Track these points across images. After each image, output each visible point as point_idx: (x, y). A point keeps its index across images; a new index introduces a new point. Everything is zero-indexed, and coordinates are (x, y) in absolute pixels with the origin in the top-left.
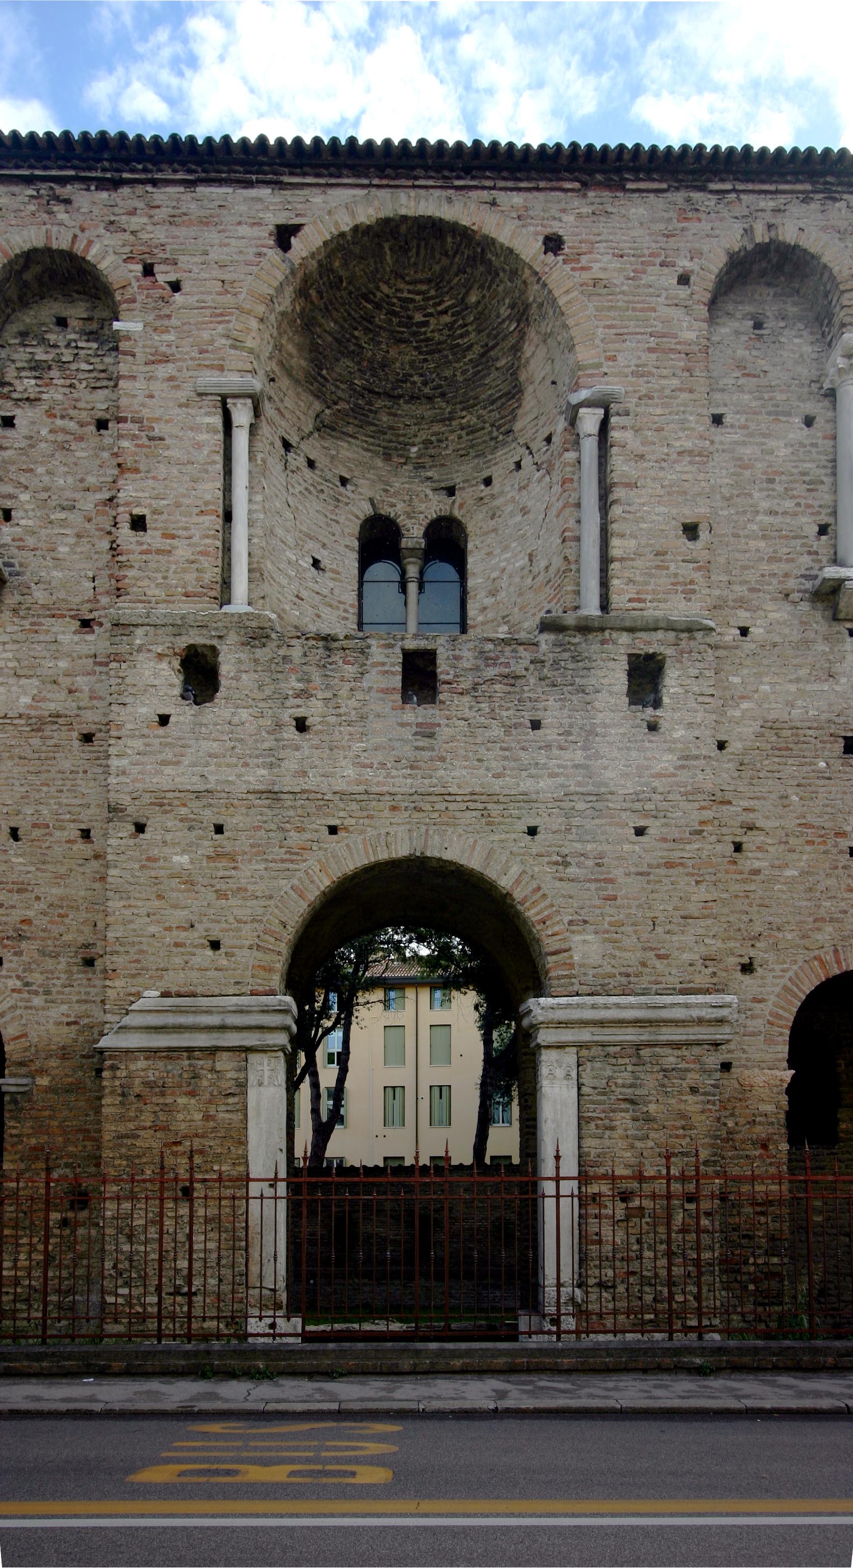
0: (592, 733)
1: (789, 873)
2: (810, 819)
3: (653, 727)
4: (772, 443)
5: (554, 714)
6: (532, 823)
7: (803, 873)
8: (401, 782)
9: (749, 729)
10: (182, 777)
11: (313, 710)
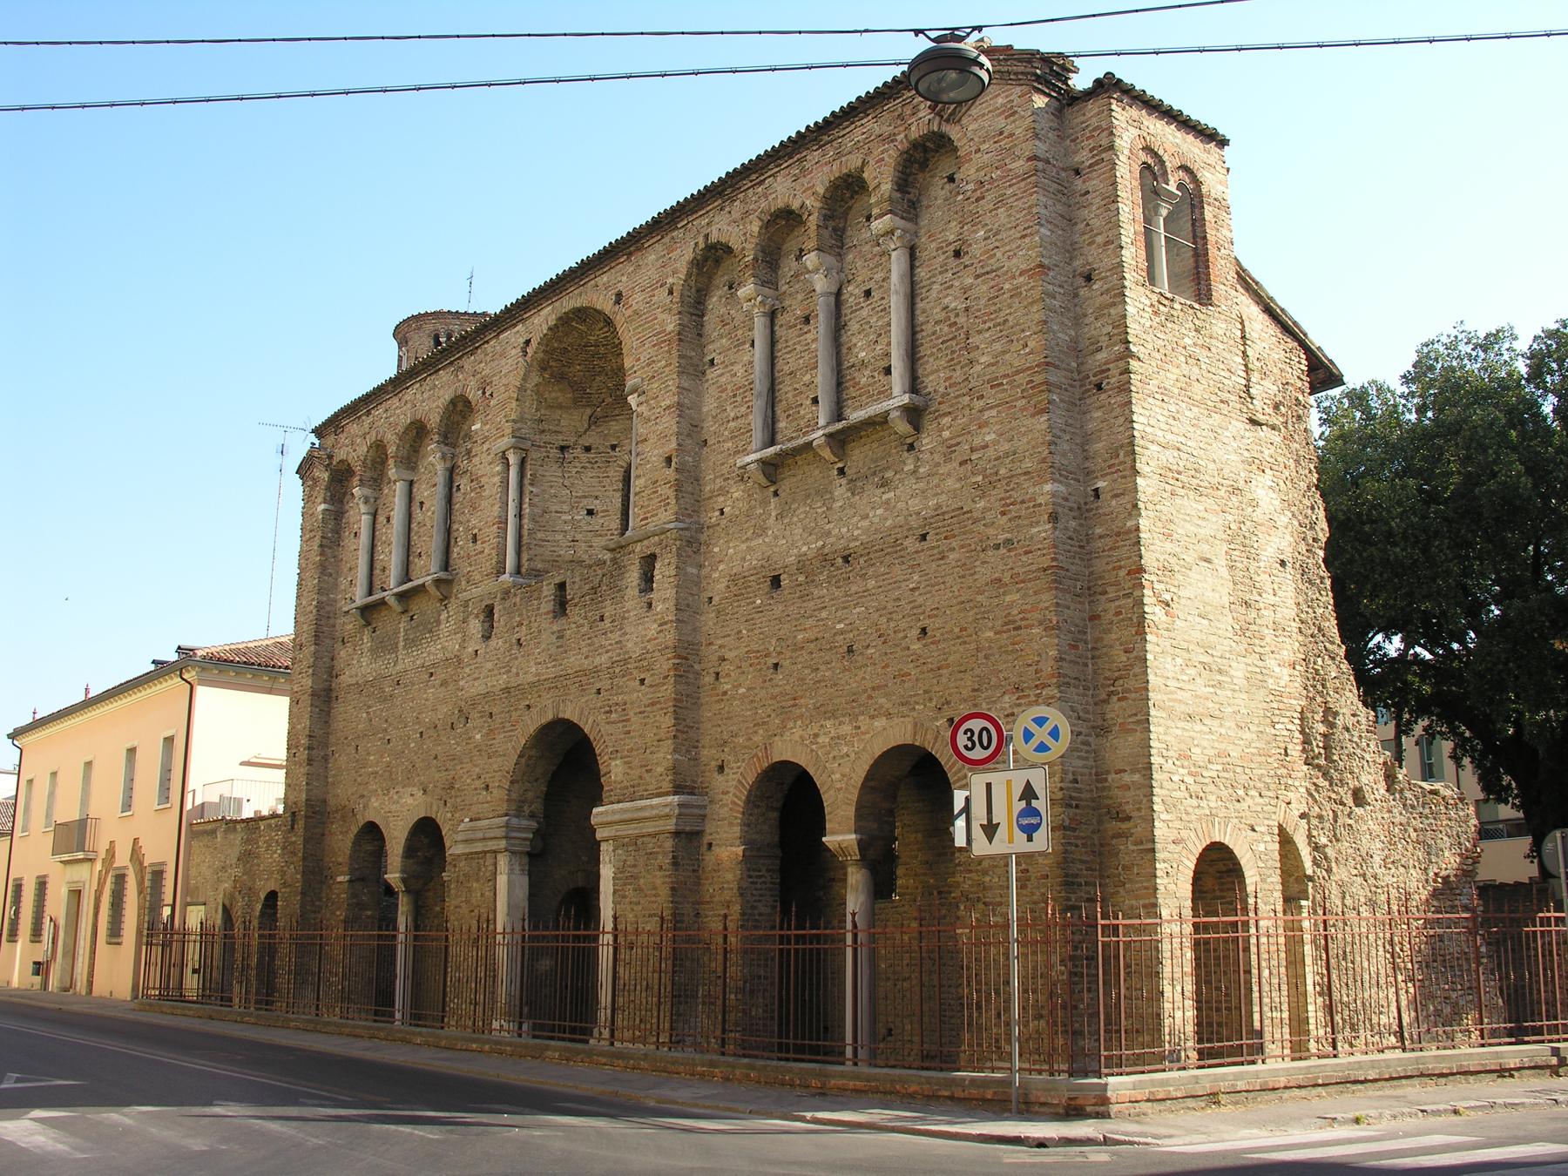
0: (624, 618)
1: (742, 690)
2: (754, 647)
3: (650, 605)
4: (736, 368)
5: (608, 610)
6: (598, 686)
7: (749, 689)
8: (551, 672)
9: (721, 586)
10: (478, 688)
11: (522, 633)
